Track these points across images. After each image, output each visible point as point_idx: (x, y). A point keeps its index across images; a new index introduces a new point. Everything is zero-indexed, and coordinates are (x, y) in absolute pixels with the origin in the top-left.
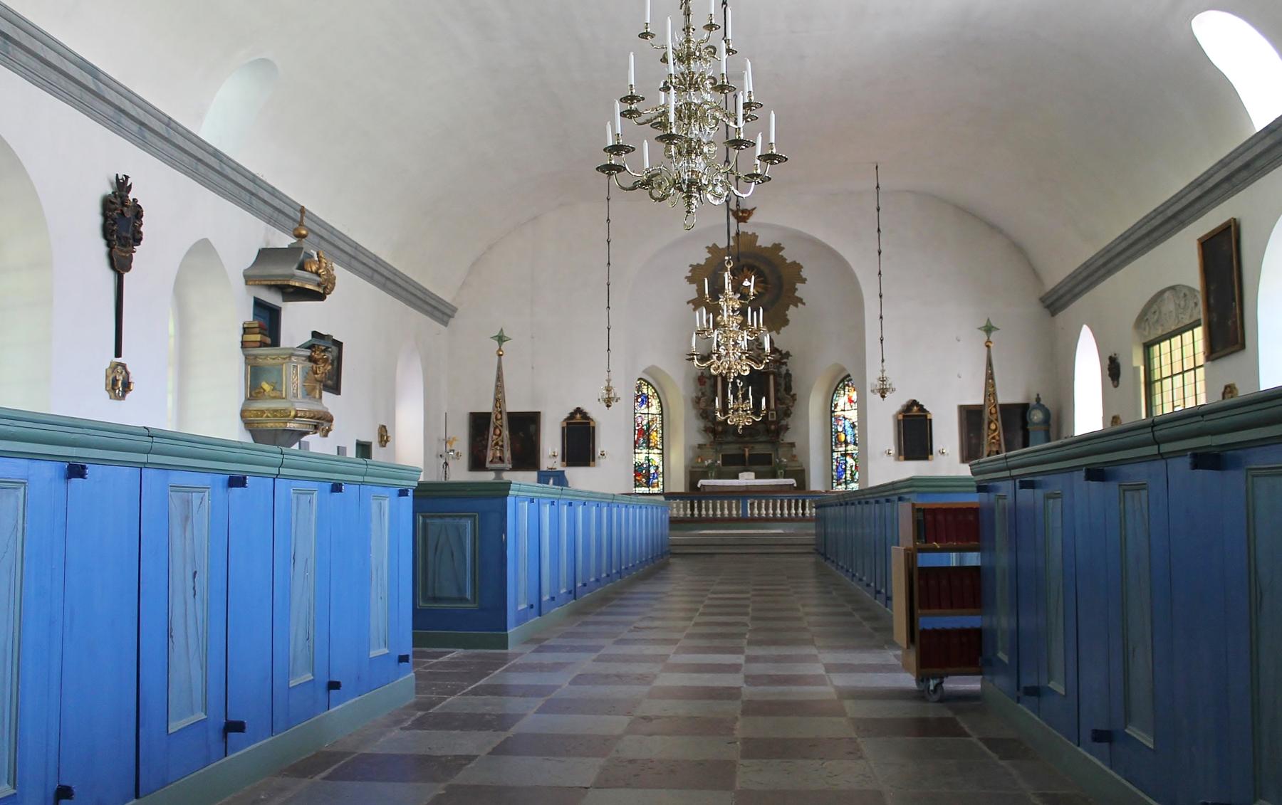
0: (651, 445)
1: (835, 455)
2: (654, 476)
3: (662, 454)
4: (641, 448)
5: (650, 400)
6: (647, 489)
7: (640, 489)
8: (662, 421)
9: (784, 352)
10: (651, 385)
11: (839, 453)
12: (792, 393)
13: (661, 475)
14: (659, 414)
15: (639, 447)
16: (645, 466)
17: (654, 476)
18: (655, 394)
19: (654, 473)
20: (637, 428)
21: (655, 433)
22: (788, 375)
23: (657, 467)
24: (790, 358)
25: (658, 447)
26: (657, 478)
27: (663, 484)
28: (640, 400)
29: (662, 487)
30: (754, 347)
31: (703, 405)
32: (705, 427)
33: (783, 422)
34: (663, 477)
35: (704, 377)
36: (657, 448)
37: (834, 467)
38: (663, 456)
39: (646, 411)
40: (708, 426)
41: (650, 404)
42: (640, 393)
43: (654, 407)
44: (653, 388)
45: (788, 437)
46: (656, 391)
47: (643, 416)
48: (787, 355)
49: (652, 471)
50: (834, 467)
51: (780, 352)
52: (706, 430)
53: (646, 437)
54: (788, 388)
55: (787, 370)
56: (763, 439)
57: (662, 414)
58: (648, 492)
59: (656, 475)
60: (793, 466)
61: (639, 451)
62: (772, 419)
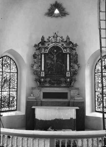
0: (11, 87)
1: (97, 93)
2: (12, 102)
3: (17, 91)
4: (5, 89)
5: (11, 66)
6: (8, 108)
7: (4, 109)
8: (17, 76)
9: (74, 44)
10: (12, 59)
11: (99, 93)
12: (78, 64)
13: (16, 101)
14: (16, 73)
15: (4, 88)
16: (7, 97)
17: (12, 102)
18: (14, 63)
19: (12, 100)
20: (3, 79)
21: (13, 81)
22: (76, 54)
23: (14, 97)
24: (77, 46)
25: (15, 88)
26: (13, 103)
27: (17, 105)
28: (5, 66)
29: (16, 106)
30: (60, 41)
31: (35, 68)
32: (36, 79)
33: (74, 78)
34: (17, 102)
35: (36, 55)
36: (14, 89)
37: (96, 99)
38: (17, 92)
39: (9, 71)
40: (37, 78)
41: (11, 68)
42: (6, 62)
43: (13, 69)
44: (13, 60)
45: (77, 85)
46: (14, 62)
47: (7, 73)
48: (76, 45)
49: (11, 99)
50: (96, 99)
51: (73, 44)
52: (36, 80)
53: (8, 83)
54: (76, 62)
55: (76, 53)
56: (64, 85)
57: (17, 73)
58: (8, 110)
59: (13, 101)
60: (78, 99)
61: (4, 90)
62: (68, 76)
